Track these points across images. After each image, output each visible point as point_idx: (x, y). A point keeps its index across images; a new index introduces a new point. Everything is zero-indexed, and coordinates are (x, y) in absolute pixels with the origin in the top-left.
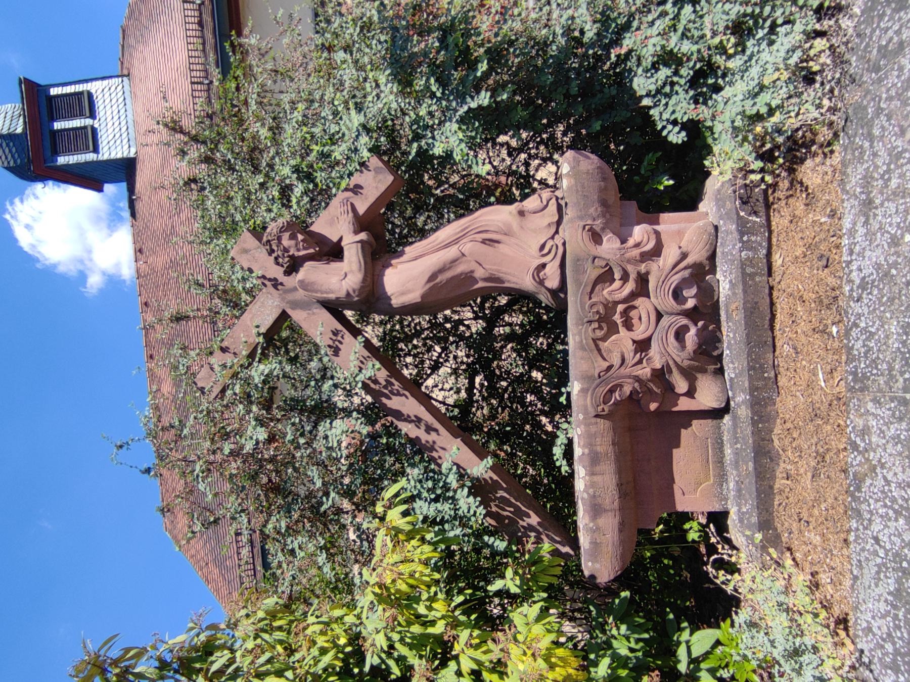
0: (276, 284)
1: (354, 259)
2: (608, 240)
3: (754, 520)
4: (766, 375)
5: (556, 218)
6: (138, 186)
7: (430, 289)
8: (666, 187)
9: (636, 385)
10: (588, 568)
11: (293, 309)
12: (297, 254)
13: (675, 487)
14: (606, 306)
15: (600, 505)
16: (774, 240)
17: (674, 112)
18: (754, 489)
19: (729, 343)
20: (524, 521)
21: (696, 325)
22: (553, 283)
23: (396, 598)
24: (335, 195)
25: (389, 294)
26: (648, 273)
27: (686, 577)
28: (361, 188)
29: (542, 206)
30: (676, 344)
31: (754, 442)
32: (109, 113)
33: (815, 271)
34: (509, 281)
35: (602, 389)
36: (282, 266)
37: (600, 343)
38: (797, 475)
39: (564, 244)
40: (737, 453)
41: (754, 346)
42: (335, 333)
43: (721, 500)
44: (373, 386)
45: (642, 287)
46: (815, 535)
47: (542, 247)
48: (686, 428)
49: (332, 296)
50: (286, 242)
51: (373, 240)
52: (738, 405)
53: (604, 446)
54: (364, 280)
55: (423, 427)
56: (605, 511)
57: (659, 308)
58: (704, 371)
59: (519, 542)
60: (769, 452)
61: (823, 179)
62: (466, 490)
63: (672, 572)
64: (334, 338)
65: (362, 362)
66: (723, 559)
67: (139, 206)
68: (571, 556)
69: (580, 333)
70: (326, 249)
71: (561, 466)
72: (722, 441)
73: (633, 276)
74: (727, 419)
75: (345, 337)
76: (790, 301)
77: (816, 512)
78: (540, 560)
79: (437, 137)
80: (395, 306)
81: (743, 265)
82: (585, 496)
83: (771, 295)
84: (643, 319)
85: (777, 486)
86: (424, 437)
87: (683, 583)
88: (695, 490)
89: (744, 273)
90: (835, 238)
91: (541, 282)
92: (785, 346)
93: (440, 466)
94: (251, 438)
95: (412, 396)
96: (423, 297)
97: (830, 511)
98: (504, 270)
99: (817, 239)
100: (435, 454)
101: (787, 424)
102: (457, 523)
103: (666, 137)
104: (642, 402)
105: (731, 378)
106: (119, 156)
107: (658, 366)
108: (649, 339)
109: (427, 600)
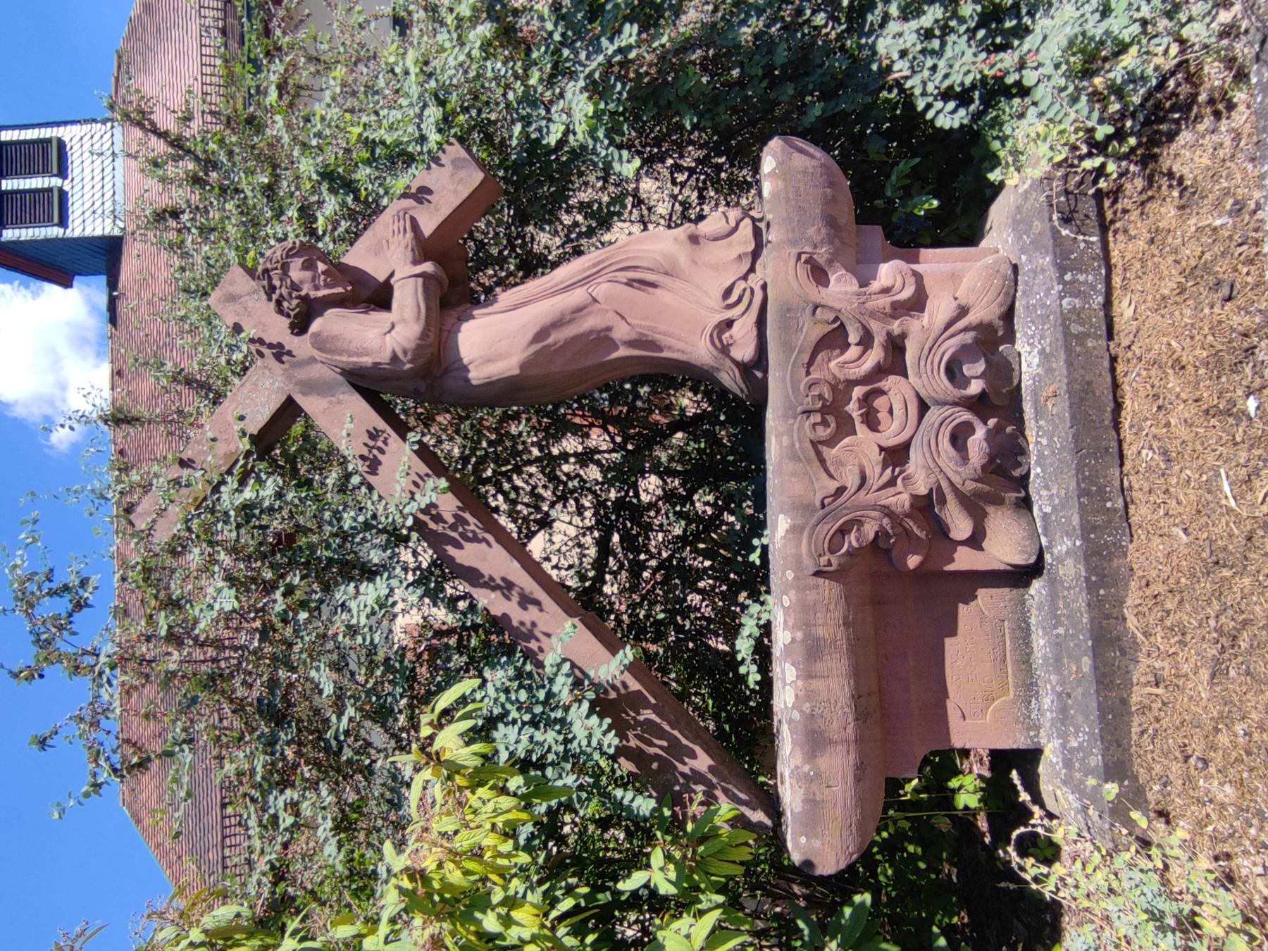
0: (280, 352)
1: (410, 302)
2: (839, 280)
3: (1096, 760)
4: (1109, 505)
5: (752, 246)
6: (123, 278)
7: (536, 353)
8: (927, 211)
9: (886, 521)
10: (797, 848)
11: (304, 394)
12: (313, 294)
13: (950, 704)
14: (834, 388)
15: (822, 732)
16: (1117, 281)
17: (946, 76)
18: (1095, 705)
19: (1041, 455)
20: (685, 764)
21: (985, 423)
22: (744, 351)
23: (443, 900)
24: (385, 207)
25: (466, 361)
26: (903, 336)
27: (949, 875)
28: (430, 192)
29: (727, 228)
30: (952, 452)
31: (1092, 620)
32: (87, 171)
33: (1207, 311)
34: (670, 348)
35: (826, 527)
36: (288, 316)
37: (824, 450)
38: (1177, 676)
39: (764, 287)
40: (1057, 644)
41: (1087, 456)
42: (374, 435)
43: (1028, 729)
44: (432, 525)
46: (1221, 784)
47: (728, 292)
48: (967, 603)
49: (367, 361)
50: (296, 273)
51: (444, 276)
52: (1060, 560)
53: (830, 627)
54: (424, 335)
55: (515, 598)
56: (832, 742)
57: (923, 393)
58: (999, 502)
59: (677, 801)
60: (1119, 639)
61: (1213, 156)
62: (586, 705)
63: (922, 865)
64: (371, 443)
65: (416, 484)
66: (1036, 835)
67: (123, 309)
68: (766, 827)
69: (790, 431)
70: (366, 294)
71: (748, 673)
72: (1028, 625)
73: (879, 339)
74: (1037, 586)
75: (390, 441)
76: (1153, 372)
77: (1223, 739)
78: (713, 835)
79: (555, 117)
80: (474, 382)
81: (1065, 320)
82: (796, 715)
83: (1113, 370)
84: (895, 412)
85: (1135, 699)
86: (517, 615)
87: (945, 887)
88: (984, 711)
89: (1067, 333)
90: (1245, 247)
91: (725, 350)
92: (1144, 452)
93: (540, 665)
94: (211, 607)
95: (498, 541)
96: (524, 366)
97: (1256, 736)
98: (663, 328)
99: (1207, 256)
100: (533, 645)
101: (1152, 587)
102: (568, 766)
103: (932, 121)
104: (894, 553)
105: (1045, 514)
106: (98, 233)
107: (923, 491)
108: (906, 446)
109: (502, 903)
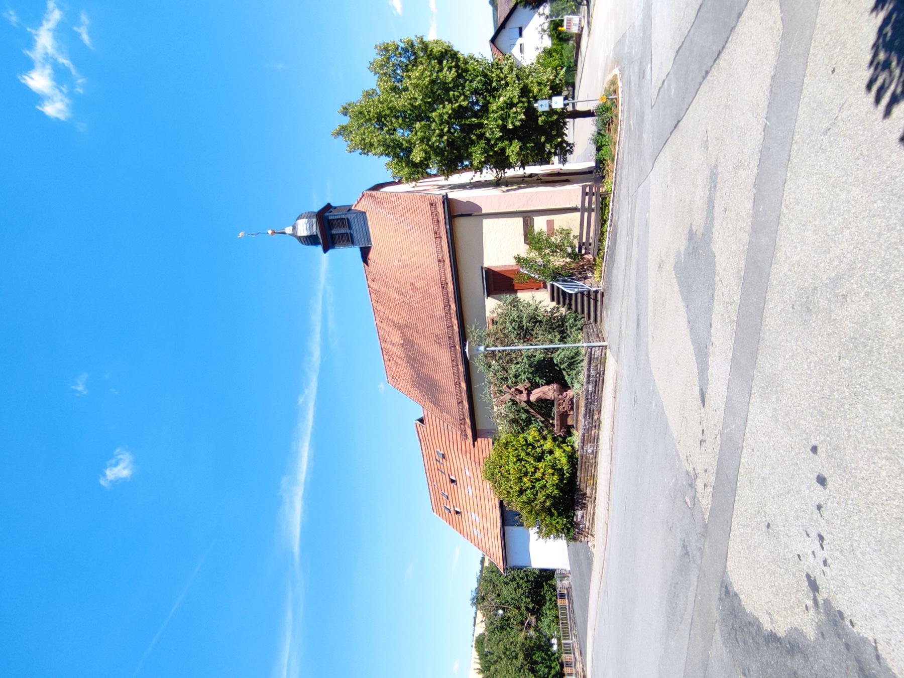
32: (357, 227)
45: (564, 401)
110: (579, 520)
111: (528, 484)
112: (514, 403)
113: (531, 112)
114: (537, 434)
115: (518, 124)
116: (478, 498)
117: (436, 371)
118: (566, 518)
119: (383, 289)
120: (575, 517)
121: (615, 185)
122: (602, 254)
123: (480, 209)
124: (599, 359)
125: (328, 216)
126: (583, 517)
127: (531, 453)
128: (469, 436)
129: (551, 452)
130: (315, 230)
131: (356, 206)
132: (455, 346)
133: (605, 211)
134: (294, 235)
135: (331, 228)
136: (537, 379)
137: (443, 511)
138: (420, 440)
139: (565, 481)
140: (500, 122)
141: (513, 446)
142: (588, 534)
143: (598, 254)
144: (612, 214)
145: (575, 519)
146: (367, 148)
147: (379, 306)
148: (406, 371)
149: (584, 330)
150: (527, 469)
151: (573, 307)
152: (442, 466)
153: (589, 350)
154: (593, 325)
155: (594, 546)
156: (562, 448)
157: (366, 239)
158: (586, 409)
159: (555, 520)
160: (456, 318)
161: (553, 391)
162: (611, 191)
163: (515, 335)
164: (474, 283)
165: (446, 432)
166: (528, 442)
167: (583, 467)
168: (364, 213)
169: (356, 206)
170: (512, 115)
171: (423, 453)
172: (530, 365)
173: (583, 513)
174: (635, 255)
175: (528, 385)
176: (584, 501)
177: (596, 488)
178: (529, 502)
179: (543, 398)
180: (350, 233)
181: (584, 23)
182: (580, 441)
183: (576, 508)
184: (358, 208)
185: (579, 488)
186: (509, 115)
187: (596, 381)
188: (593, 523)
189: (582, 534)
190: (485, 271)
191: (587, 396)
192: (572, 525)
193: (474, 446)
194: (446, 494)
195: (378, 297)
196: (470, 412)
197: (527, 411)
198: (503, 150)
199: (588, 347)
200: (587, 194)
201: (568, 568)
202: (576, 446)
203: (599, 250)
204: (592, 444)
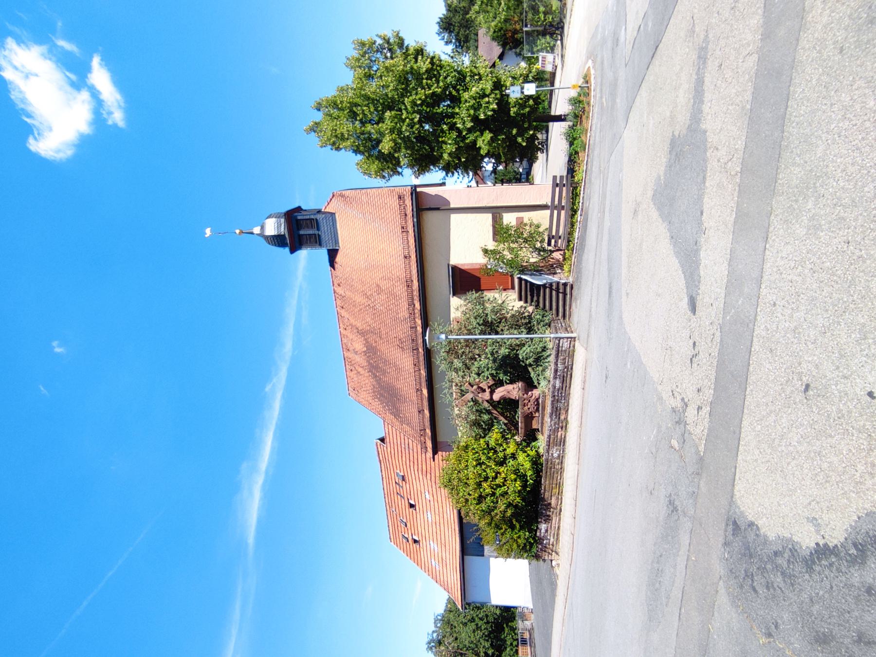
32: (326, 229)
45: (529, 401)
53: (523, 421)
110: (542, 535)
111: (488, 491)
112: (475, 402)
113: (503, 102)
114: (500, 435)
115: (490, 113)
116: (438, 524)
117: (397, 379)
118: (528, 532)
119: (348, 294)
120: (538, 531)
121: (586, 172)
122: (572, 246)
123: (448, 203)
124: (567, 352)
125: (296, 216)
126: (547, 531)
127: (493, 457)
128: (429, 448)
129: (514, 456)
130: (282, 229)
131: (326, 208)
132: (418, 349)
133: (576, 200)
134: (262, 235)
135: (299, 229)
136: (501, 376)
137: (401, 540)
138: (380, 461)
139: (528, 489)
140: (472, 112)
141: (474, 449)
142: (553, 551)
143: (568, 246)
144: (582, 203)
145: (538, 534)
146: (336, 141)
147: (343, 313)
148: (367, 381)
149: (552, 324)
150: (487, 474)
151: (541, 305)
152: (401, 489)
153: (557, 342)
154: (562, 320)
155: (558, 565)
156: (525, 452)
157: (334, 241)
158: (553, 407)
159: (516, 533)
160: (420, 318)
161: (518, 389)
162: (582, 180)
163: (479, 331)
164: (441, 281)
165: (407, 451)
166: (490, 446)
167: (548, 473)
168: (333, 214)
169: (326, 208)
170: (484, 105)
171: (382, 475)
172: (494, 361)
173: (548, 527)
174: (607, 224)
175: (491, 382)
176: (548, 513)
177: (562, 498)
178: (489, 511)
179: (507, 397)
180: (318, 234)
181: (558, 62)
182: (545, 445)
183: (540, 520)
184: (327, 210)
185: (544, 498)
186: (481, 105)
187: (564, 376)
188: (558, 539)
189: (545, 551)
190: (452, 268)
191: (553, 392)
192: (535, 541)
193: (434, 460)
194: (404, 520)
195: (343, 302)
196: (431, 420)
197: (489, 412)
198: (474, 142)
199: (556, 338)
200: (557, 185)
201: (531, 606)
202: (541, 451)
203: (569, 241)
204: (558, 447)
